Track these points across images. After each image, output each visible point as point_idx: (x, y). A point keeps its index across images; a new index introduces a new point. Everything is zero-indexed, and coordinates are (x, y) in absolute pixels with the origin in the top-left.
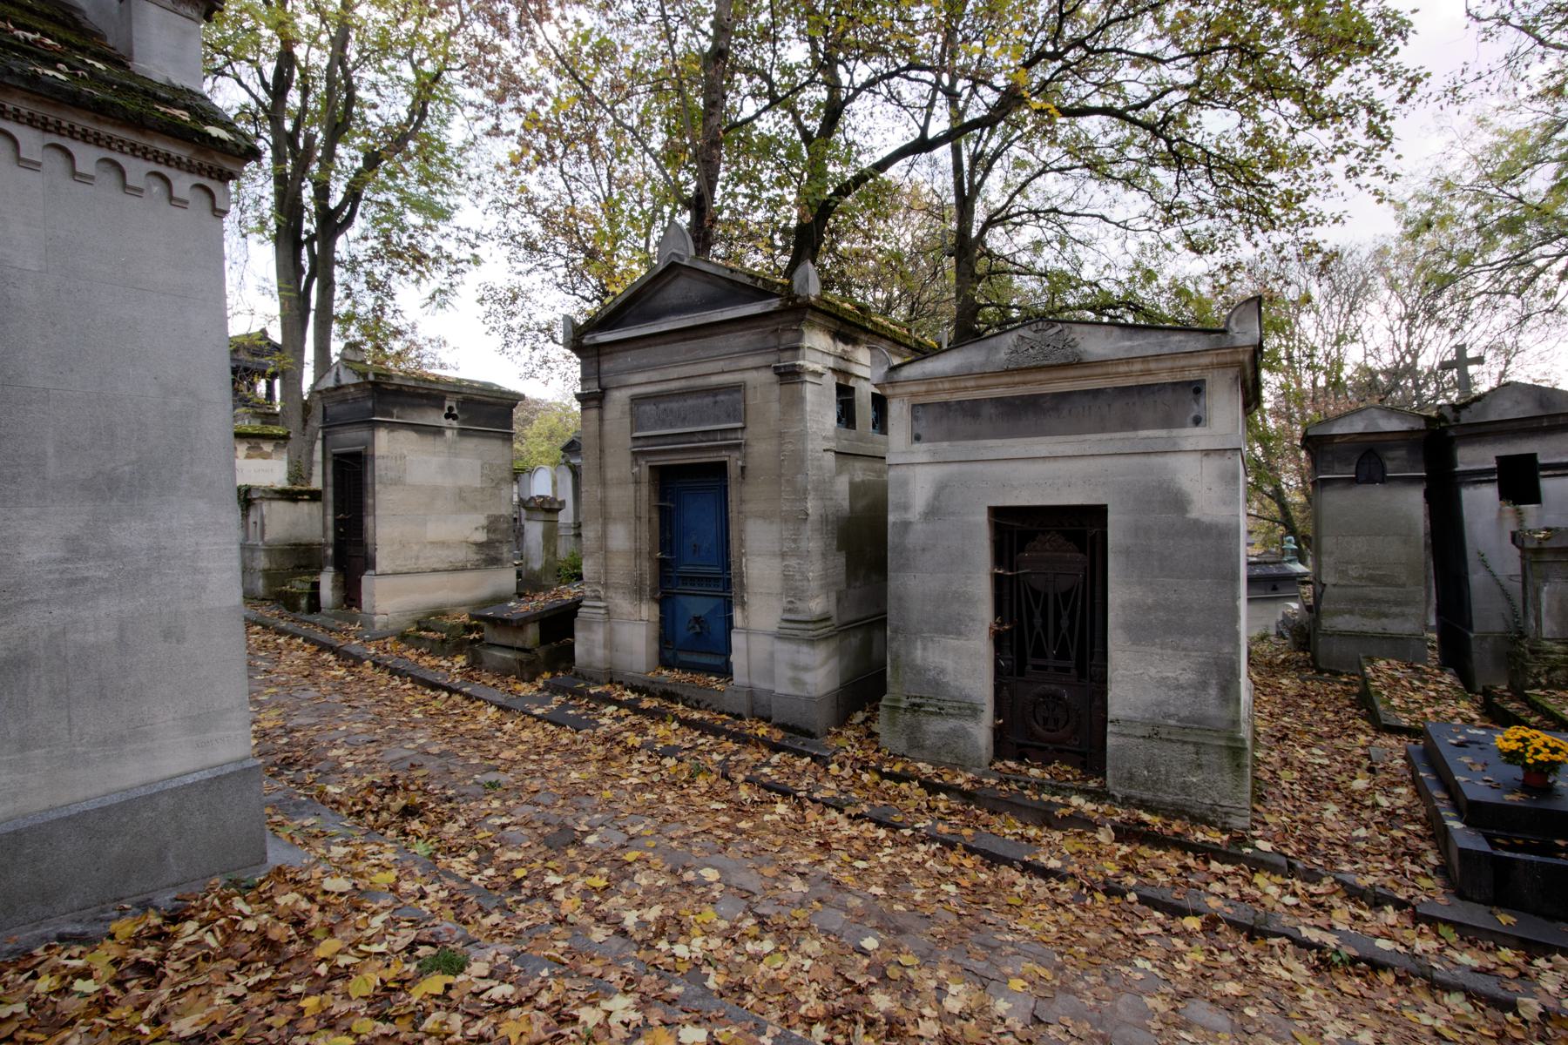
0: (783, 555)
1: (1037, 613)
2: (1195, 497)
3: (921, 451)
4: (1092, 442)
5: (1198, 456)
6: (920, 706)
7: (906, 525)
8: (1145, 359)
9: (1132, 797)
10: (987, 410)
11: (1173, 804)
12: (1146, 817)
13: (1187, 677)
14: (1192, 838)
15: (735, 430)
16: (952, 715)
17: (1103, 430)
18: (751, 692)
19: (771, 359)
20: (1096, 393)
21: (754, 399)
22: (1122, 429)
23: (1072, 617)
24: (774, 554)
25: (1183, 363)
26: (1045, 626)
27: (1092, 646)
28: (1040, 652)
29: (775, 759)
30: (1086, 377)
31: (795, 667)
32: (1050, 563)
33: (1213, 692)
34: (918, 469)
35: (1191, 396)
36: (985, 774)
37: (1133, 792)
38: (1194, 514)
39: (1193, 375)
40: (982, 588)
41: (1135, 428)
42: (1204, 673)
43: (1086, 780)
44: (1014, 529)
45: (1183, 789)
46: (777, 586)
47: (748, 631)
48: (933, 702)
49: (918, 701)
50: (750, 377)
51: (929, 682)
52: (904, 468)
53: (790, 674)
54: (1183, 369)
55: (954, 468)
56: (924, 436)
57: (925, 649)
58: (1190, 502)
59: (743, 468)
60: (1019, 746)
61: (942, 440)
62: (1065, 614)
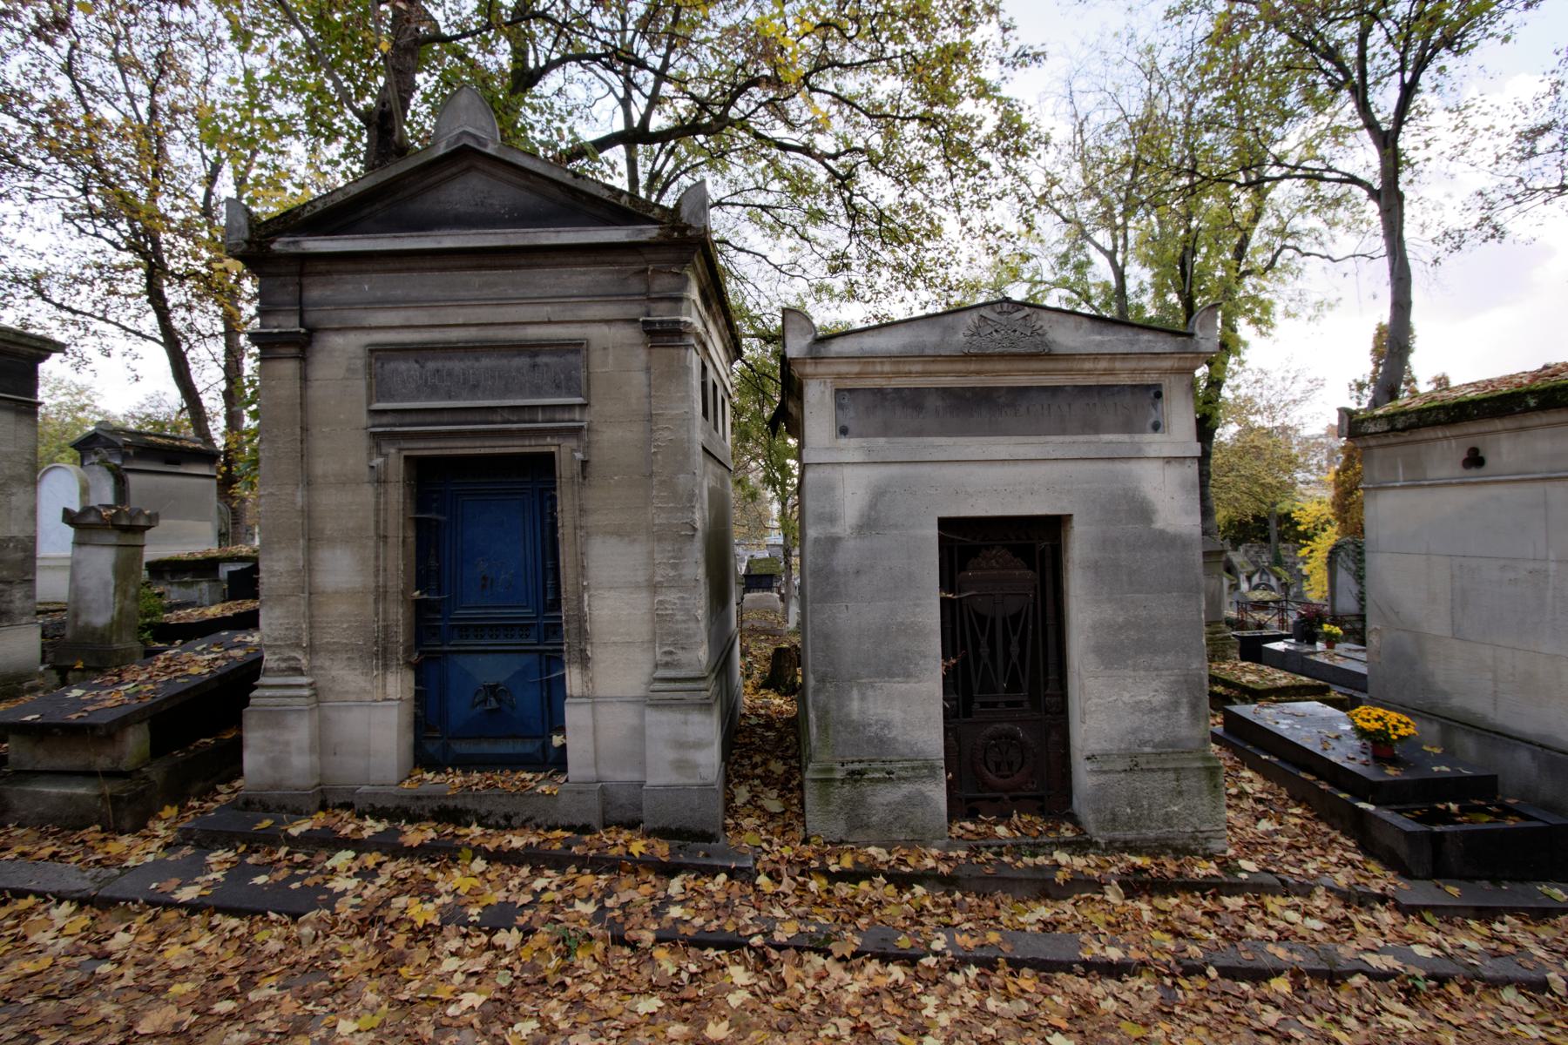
0: (654, 587)
1: (984, 641)
2: (1159, 506)
3: (851, 449)
4: (1054, 444)
5: (1160, 464)
6: (861, 773)
7: (833, 542)
8: (1113, 356)
9: (1115, 841)
10: (932, 402)
12: (1139, 861)
13: (1160, 698)
14: (1193, 875)
15: (570, 407)
16: (906, 779)
17: (1064, 432)
18: (605, 793)
19: (635, 310)
20: (1055, 390)
21: (602, 366)
22: (1083, 433)
24: (637, 587)
25: (1146, 364)
27: (1046, 674)
29: (675, 886)
30: (1047, 372)
31: (681, 745)
33: (1184, 711)
34: (847, 470)
36: (950, 847)
37: (1117, 834)
38: (1159, 525)
39: (1149, 379)
40: (931, 617)
41: (1097, 431)
43: (1056, 829)
44: (964, 541)
45: (1165, 821)
46: (642, 631)
47: (592, 699)
48: (874, 765)
49: (857, 766)
50: (595, 333)
51: (869, 741)
52: (828, 469)
53: (671, 755)
54: (1143, 371)
55: (894, 470)
57: (863, 698)
58: (1154, 512)
59: (584, 463)
60: (969, 800)
62: (1015, 639)
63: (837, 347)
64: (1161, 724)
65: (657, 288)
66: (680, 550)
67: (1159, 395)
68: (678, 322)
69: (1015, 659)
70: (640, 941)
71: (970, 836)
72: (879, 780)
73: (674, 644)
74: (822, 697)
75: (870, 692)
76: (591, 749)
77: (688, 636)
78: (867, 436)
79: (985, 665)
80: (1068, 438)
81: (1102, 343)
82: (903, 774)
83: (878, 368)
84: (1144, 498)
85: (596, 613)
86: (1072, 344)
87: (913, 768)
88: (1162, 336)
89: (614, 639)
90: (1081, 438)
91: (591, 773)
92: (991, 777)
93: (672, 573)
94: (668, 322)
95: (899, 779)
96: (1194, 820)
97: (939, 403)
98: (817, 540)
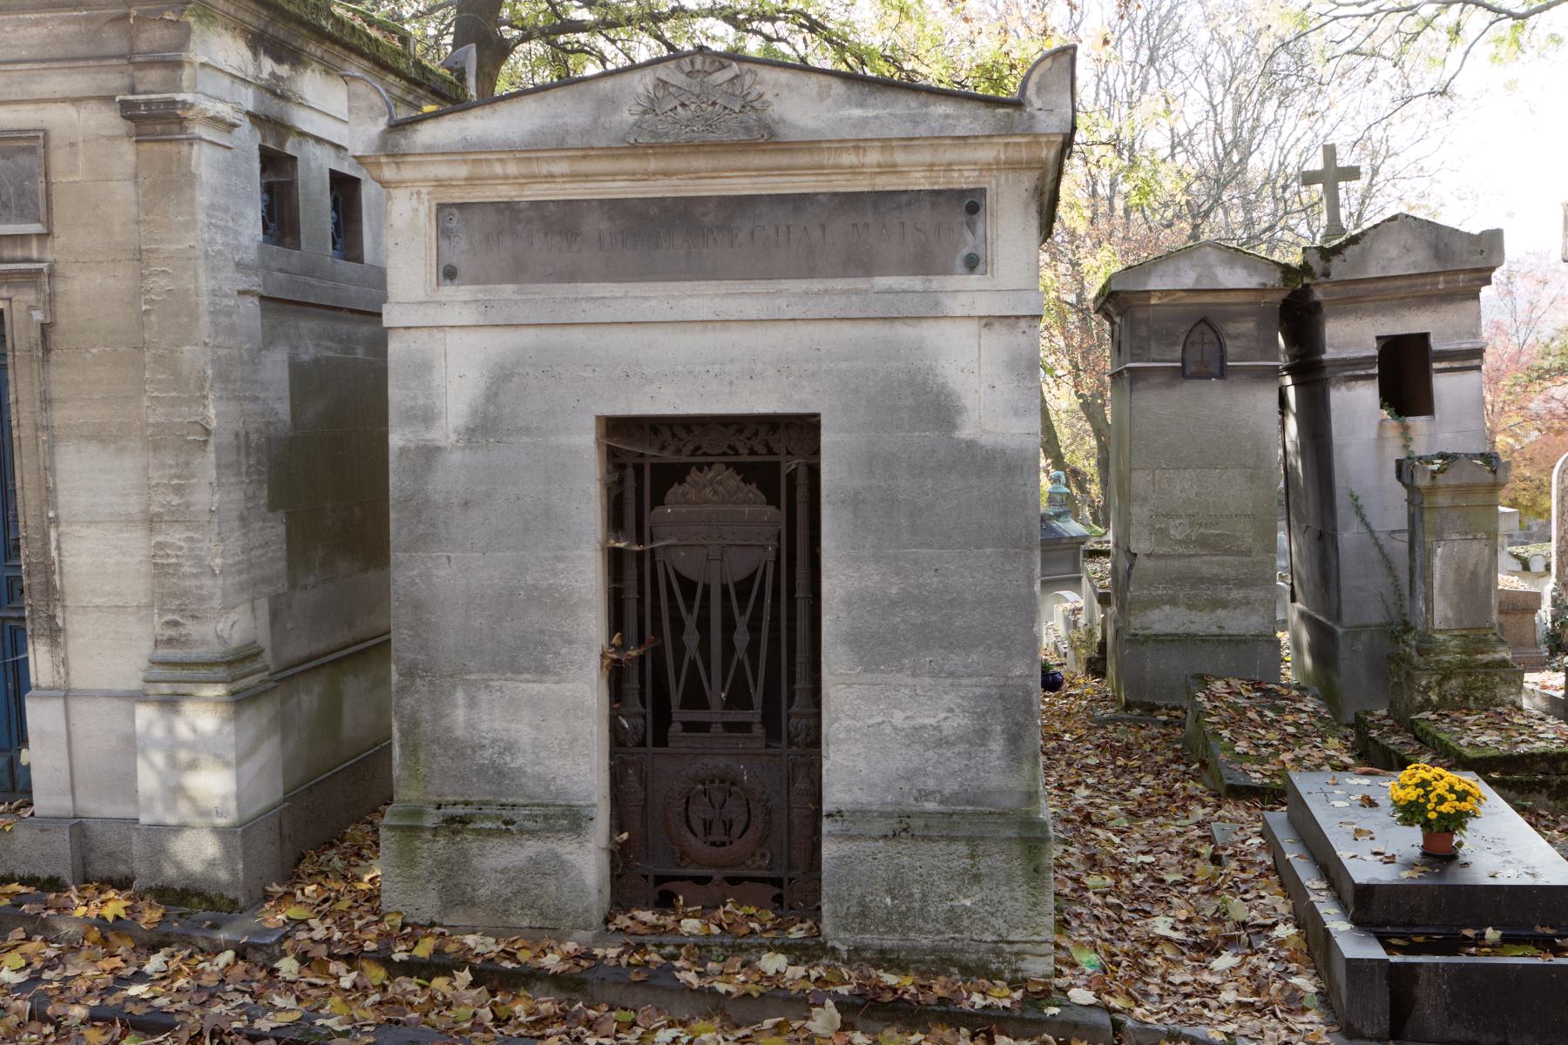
0: (152, 522)
1: (690, 622)
2: (968, 401)
3: (459, 303)
4: (791, 294)
5: (973, 326)
6: (464, 821)
7: (429, 454)
8: (886, 143)
9: (866, 948)
10: (594, 225)
11: (934, 950)
12: (890, 979)
13: (957, 723)
14: (966, 1006)
15: (24, 238)
16: (532, 833)
17: (812, 273)
18: (79, 827)
19: (113, 81)
21: (68, 172)
22: (845, 274)
23: (754, 627)
24: (128, 521)
25: (949, 155)
26: (704, 647)
27: (792, 680)
28: (695, 697)
29: (155, 963)
30: (782, 170)
32: (713, 526)
33: (997, 746)
34: (453, 338)
35: (962, 218)
36: (600, 939)
37: (870, 938)
38: (966, 432)
39: (964, 179)
40: (586, 577)
41: (868, 270)
43: (782, 928)
44: (649, 460)
45: (949, 922)
46: (137, 588)
47: (67, 694)
48: (486, 810)
49: (459, 811)
50: (57, 118)
51: (481, 771)
52: (423, 336)
55: (528, 337)
57: (472, 704)
58: (960, 410)
59: (45, 329)
60: (660, 880)
61: (502, 281)
64: (956, 765)
65: (143, 46)
66: (187, 464)
67: (973, 209)
68: (174, 102)
69: (740, 653)
70: (66, 1017)
71: (641, 929)
72: (490, 833)
73: (181, 610)
74: (409, 701)
75: (483, 696)
76: (65, 764)
77: (201, 599)
79: (740, 663)
80: (816, 285)
81: (864, 121)
82: (530, 825)
83: (498, 169)
84: (943, 386)
85: (68, 560)
86: (811, 124)
87: (546, 817)
88: (969, 107)
89: (97, 601)
90: (840, 284)
91: (63, 805)
92: (695, 844)
93: (176, 501)
94: (158, 103)
95: (521, 832)
96: (998, 923)
97: (605, 225)
98: (403, 451)
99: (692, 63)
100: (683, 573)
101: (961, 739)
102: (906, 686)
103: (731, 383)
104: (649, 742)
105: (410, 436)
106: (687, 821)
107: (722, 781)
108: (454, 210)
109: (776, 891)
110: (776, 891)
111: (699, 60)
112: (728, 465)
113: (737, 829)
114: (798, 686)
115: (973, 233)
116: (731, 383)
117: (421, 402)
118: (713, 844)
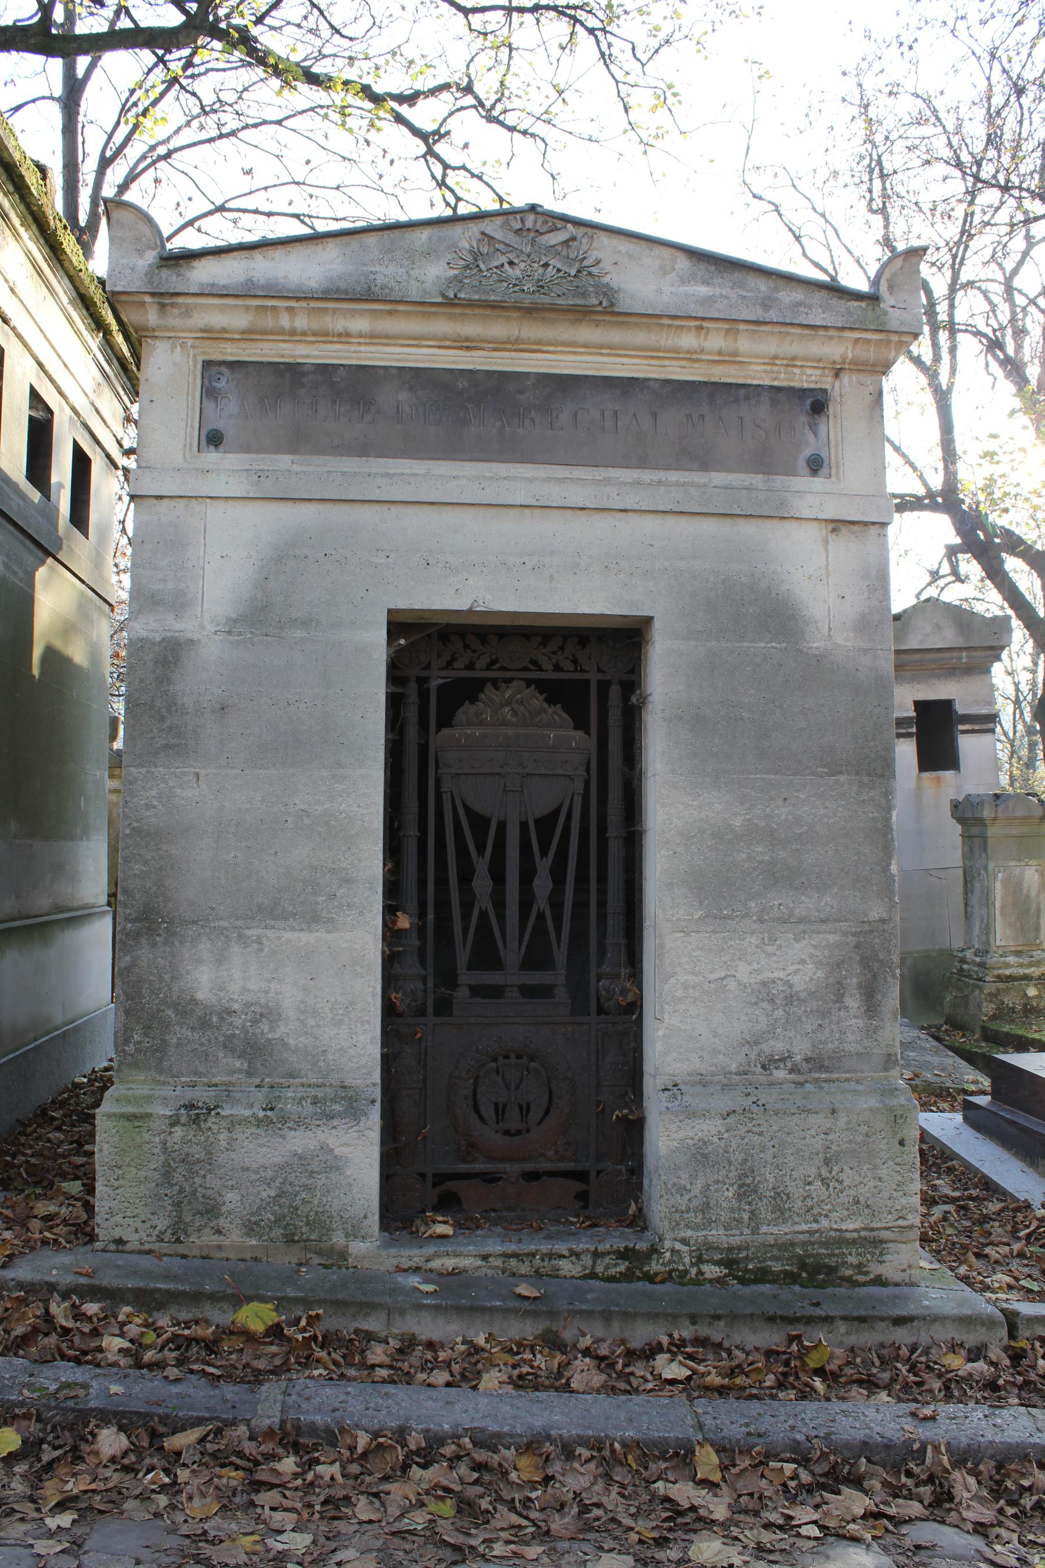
1: (482, 865)
3: (226, 473)
4: (621, 483)
9: (711, 1247)
16: (300, 1123)
17: (643, 463)
20: (627, 386)
23: (558, 874)
25: (795, 348)
28: (486, 956)
30: (613, 349)
33: (853, 1002)
34: (215, 512)
35: (803, 419)
38: (817, 644)
39: (805, 379)
42: (839, 965)
44: (444, 668)
54: (792, 361)
56: (229, 435)
57: (221, 959)
60: (440, 1178)
61: (278, 450)
62: (543, 866)
63: (203, 273)
69: (542, 903)
75: (235, 949)
78: (260, 450)
80: (647, 475)
83: (285, 321)
90: (673, 476)
97: (403, 396)
99: (522, 221)
100: (475, 806)
101: (812, 994)
102: (753, 933)
103: (551, 577)
104: (430, 1010)
105: (154, 625)
106: (477, 1111)
107: (519, 1057)
108: (223, 369)
109: (583, 1187)
110: (583, 1187)
111: (530, 219)
112: (529, 682)
113: (535, 1114)
114: (609, 940)
115: (816, 434)
116: (551, 577)
117: (170, 585)
118: (507, 1133)
